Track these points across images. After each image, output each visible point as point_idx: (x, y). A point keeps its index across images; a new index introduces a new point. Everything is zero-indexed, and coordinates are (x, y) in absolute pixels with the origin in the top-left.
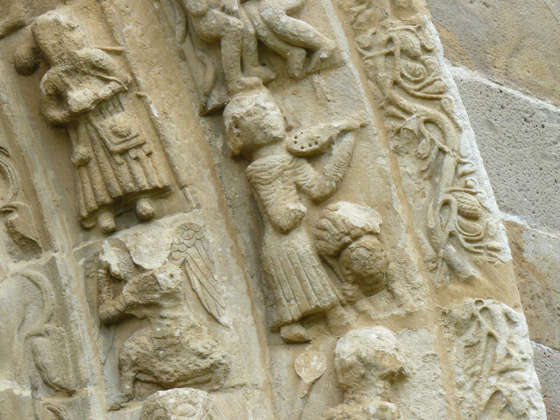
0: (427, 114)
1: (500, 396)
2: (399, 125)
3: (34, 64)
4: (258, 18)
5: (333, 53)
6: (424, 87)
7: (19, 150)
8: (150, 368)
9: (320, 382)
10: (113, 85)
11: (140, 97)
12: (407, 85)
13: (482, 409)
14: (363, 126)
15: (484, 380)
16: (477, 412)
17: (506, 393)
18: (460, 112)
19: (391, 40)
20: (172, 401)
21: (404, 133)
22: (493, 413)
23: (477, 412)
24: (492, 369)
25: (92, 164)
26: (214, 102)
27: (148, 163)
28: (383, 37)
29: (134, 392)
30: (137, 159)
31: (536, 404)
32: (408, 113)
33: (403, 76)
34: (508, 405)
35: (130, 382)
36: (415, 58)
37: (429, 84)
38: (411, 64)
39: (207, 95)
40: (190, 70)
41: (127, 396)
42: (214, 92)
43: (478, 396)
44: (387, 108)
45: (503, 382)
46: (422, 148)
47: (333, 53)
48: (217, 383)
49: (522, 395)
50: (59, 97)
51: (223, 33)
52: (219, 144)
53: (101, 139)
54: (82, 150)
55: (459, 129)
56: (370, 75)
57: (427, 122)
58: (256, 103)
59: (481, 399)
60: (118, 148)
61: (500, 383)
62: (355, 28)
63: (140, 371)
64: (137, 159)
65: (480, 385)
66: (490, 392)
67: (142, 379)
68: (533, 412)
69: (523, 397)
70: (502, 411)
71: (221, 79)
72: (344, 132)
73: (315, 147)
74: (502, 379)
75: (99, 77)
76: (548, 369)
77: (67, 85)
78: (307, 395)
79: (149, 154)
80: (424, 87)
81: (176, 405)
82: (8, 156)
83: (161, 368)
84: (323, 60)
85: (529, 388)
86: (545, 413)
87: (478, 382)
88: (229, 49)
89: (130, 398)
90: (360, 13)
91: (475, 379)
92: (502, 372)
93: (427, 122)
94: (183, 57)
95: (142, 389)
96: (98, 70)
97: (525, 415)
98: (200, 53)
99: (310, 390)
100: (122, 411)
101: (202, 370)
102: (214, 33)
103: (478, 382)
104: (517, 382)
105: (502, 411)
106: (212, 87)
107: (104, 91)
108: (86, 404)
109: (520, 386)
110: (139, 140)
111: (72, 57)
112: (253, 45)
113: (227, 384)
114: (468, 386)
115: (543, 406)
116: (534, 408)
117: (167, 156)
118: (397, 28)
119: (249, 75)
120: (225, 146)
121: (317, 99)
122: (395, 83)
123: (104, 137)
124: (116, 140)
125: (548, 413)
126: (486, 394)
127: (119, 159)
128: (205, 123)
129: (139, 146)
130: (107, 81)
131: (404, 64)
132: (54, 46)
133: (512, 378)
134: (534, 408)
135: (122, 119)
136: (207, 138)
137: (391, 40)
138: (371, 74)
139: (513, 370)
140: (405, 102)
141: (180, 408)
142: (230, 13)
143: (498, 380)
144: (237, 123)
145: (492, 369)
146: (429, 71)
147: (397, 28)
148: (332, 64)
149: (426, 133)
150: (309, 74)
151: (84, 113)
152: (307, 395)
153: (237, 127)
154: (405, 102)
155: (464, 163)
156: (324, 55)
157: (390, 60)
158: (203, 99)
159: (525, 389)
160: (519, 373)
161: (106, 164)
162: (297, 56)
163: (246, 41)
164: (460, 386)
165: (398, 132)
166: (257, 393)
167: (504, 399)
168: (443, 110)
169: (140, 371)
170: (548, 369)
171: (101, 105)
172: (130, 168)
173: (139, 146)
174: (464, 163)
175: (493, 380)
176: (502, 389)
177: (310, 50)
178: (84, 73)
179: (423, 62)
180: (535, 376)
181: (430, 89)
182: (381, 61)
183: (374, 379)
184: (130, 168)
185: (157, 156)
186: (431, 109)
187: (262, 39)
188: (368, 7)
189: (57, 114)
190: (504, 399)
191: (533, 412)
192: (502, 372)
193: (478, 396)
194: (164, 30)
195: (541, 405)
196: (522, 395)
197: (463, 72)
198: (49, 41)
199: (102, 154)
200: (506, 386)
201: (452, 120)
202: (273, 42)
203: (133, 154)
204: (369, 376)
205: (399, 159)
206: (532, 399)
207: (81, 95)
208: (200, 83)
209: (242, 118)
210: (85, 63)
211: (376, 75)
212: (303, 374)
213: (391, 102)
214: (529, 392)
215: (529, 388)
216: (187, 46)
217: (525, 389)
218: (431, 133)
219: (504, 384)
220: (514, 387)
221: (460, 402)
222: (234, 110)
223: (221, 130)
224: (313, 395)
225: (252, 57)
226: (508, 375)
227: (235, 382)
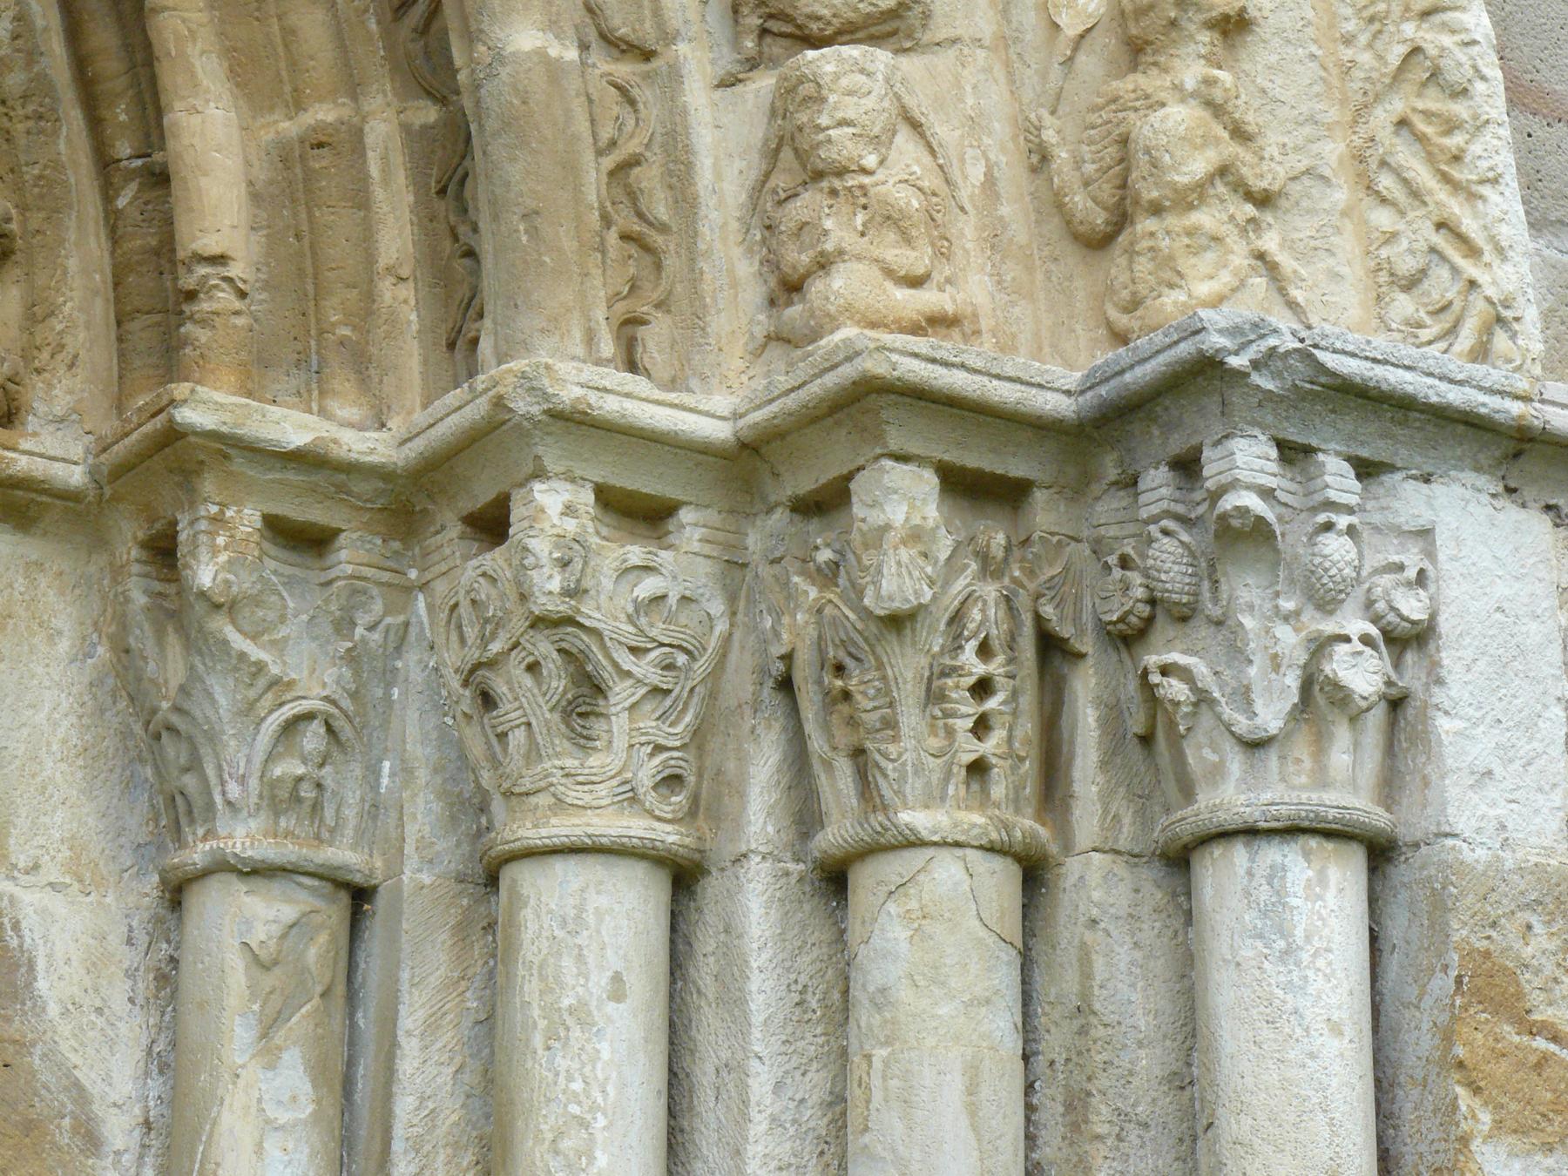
1: (1422, 57)
8: (789, 11)
9: (1094, 33)
13: (1387, 81)
15: (1392, 28)
16: (1379, 87)
17: (1432, 51)
20: (829, 68)
22: (1407, 88)
23: (1379, 87)
24: (1407, 9)
29: (761, 53)
31: (1486, 71)
34: (1435, 74)
35: (754, 36)
41: (747, 60)
43: (1380, 58)
45: (1427, 31)
48: (909, 36)
49: (1461, 55)
59: (1386, 64)
61: (1421, 34)
63: (771, 16)
65: (1385, 37)
66: (1402, 50)
67: (775, 29)
68: (1480, 87)
69: (1464, 59)
70: (1424, 85)
74: (1425, 26)
76: (1508, 8)
78: (1071, 59)
81: (837, 77)
83: (808, 10)
85: (1474, 42)
86: (1502, 87)
87: (1380, 32)
89: (753, 64)
91: (1377, 26)
92: (1426, 14)
95: (775, 47)
97: (1465, 90)
99: (1075, 49)
100: (739, 88)
101: (882, 13)
103: (1380, 32)
104: (1453, 32)
105: (1424, 85)
108: (675, 75)
109: (1457, 38)
113: (926, 38)
114: (1363, 39)
115: (1500, 75)
116: (1483, 78)
125: (1507, 89)
126: (1396, 53)
133: (1444, 24)
134: (1483, 78)
139: (1445, 9)
141: (844, 82)
143: (1419, 27)
145: (1407, 9)
152: (1071, 59)
159: (1467, 44)
160: (1457, 14)
164: (1348, 40)
166: (981, 54)
167: (1428, 63)
169: (771, 16)
170: (1508, 8)
175: (1409, 29)
176: (1424, 45)
180: (1486, 20)
183: (1192, 27)
190: (1428, 63)
191: (1480, 87)
192: (1426, 14)
193: (1380, 58)
195: (1495, 73)
196: (1461, 55)
200: (1432, 38)
204: (1183, 23)
206: (1480, 63)
212: (1063, 20)
214: (1476, 48)
215: (1474, 42)
217: (1467, 44)
219: (1428, 36)
220: (1447, 40)
221: (1347, 69)
224: (1081, 58)
226: (1437, 19)
227: (940, 36)
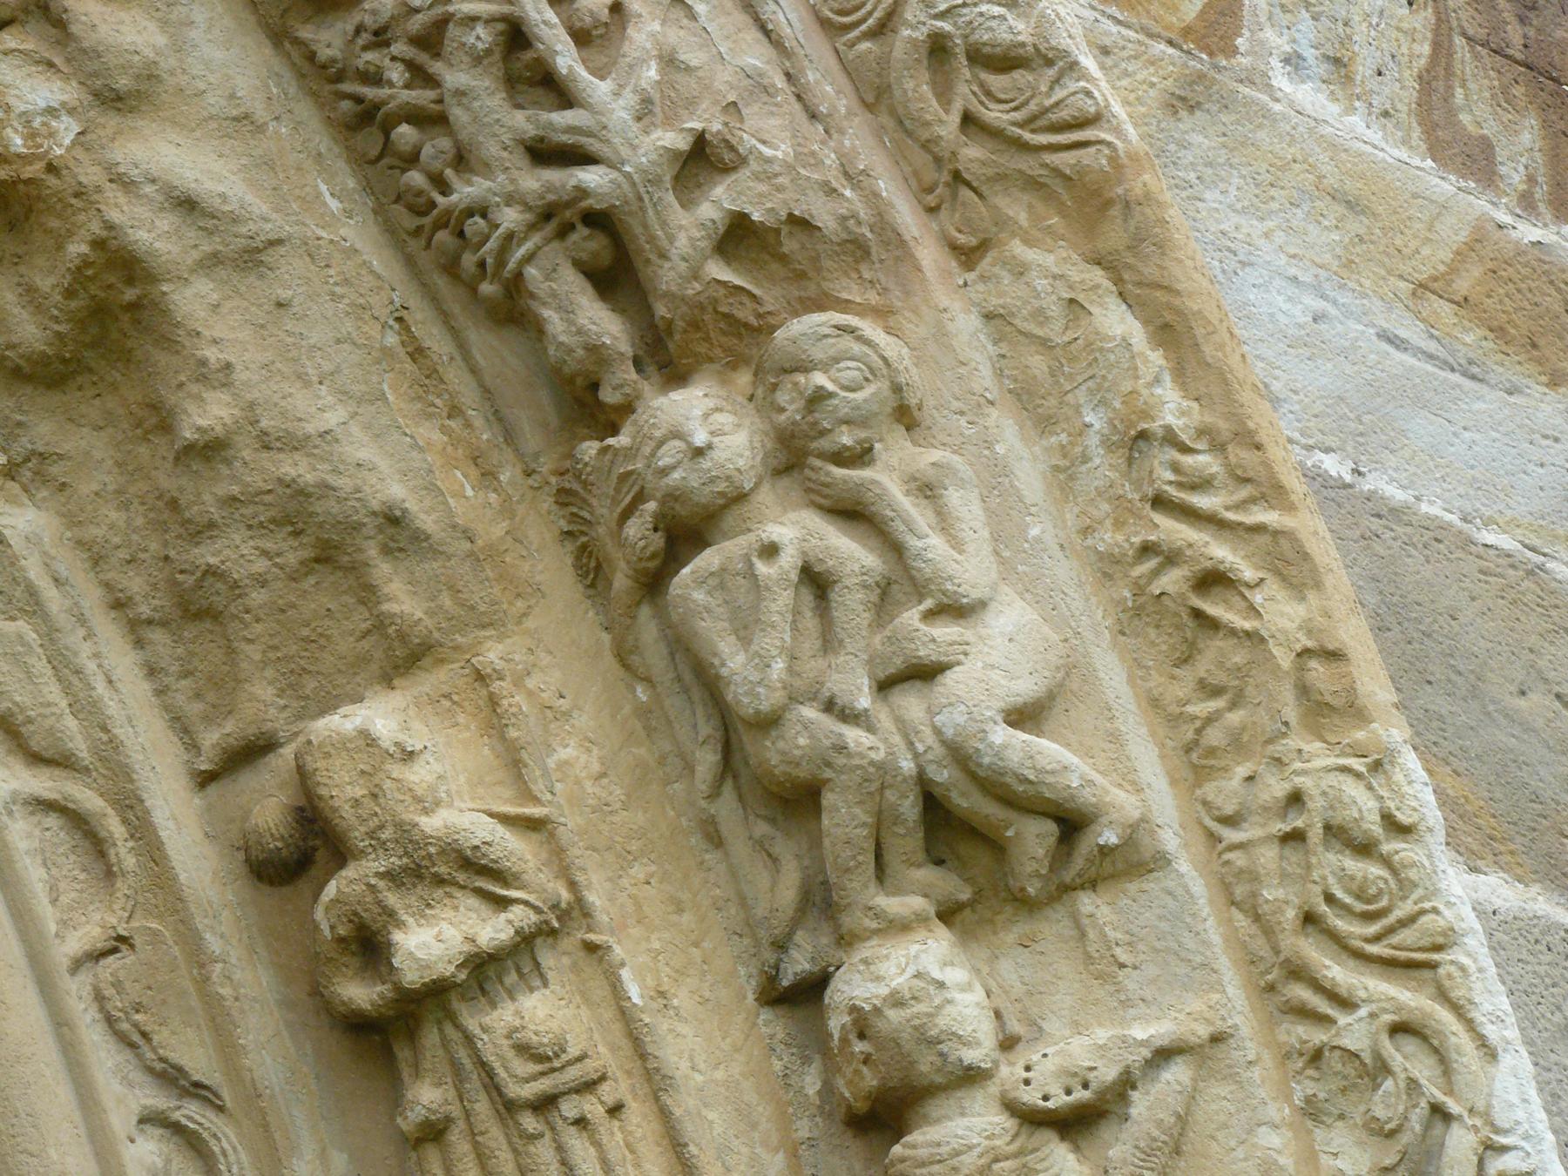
0: (1399, 1009)
2: (1319, 1036)
3: (301, 853)
4: (927, 731)
5: (1134, 833)
6: (1390, 931)
7: (253, 1096)
10: (517, 912)
11: (591, 948)
12: (1341, 924)
14: (1217, 1039)
18: (1493, 1002)
19: (1296, 799)
21: (1333, 1061)
25: (457, 1139)
26: (798, 964)
27: (613, 1136)
28: (1276, 788)
30: (581, 1122)
32: (1346, 1003)
33: (1330, 899)
36: (1365, 849)
37: (1404, 923)
38: (1353, 865)
39: (781, 946)
40: (733, 874)
42: (800, 937)
44: (1287, 989)
46: (1385, 1102)
47: (1134, 833)
50: (368, 945)
51: (828, 774)
52: (811, 1083)
53: (483, 1065)
54: (427, 1097)
55: (1489, 1052)
56: (1238, 893)
57: (1399, 1029)
58: (918, 971)
60: (528, 1091)
62: (1196, 761)
64: (581, 1122)
71: (820, 902)
72: (1164, 1055)
73: (1081, 1095)
75: (481, 893)
77: (391, 914)
79: (615, 1110)
80: (1390, 931)
82: (221, 1109)
84: (1105, 851)
88: (844, 817)
90: (1210, 720)
93: (1399, 1029)
94: (715, 839)
96: (477, 873)
98: (762, 828)
102: (802, 773)
106: (795, 923)
107: (494, 930)
110: (589, 1069)
111: (407, 836)
112: (910, 808)
117: (665, 1114)
118: (1314, 762)
119: (898, 891)
120: (827, 1089)
121: (1088, 959)
122: (1309, 919)
123: (491, 1058)
124: (526, 1068)
127: (530, 1122)
128: (773, 1025)
129: (588, 1086)
130: (502, 903)
131: (1334, 865)
132: (356, 803)
135: (541, 1010)
136: (777, 1065)
137: (1296, 799)
138: (1240, 891)
140: (1338, 972)
142: (848, 716)
144: (862, 1024)
146: (1406, 887)
147: (1314, 762)
148: (1131, 862)
149: (1396, 1059)
150: (1066, 889)
151: (437, 994)
153: (862, 1036)
154: (1338, 972)
155: (1504, 1149)
156: (1110, 837)
157: (1293, 855)
158: (769, 956)
161: (495, 1136)
162: (1033, 839)
163: (890, 796)
165: (1316, 1056)
168: (1443, 996)
171: (484, 971)
172: (560, 1148)
173: (588, 1086)
174: (1504, 1149)
177: (1070, 824)
178: (440, 881)
179: (1386, 861)
181: (1406, 936)
182: (1268, 856)
184: (560, 1148)
185: (638, 1116)
186: (1409, 994)
187: (936, 791)
188: (1233, 705)
189: (360, 993)
194: (662, 760)
197: (1501, 891)
198: (342, 789)
199: (482, 1107)
201: (1470, 1025)
202: (967, 800)
203: (569, 1108)
205: (1319, 1134)
207: (430, 941)
208: (760, 912)
209: (877, 1010)
210: (442, 852)
211: (1254, 895)
213: (1298, 972)
216: (727, 808)
218: (1408, 1060)
222: (853, 988)
223: (816, 1043)
225: (907, 840)
